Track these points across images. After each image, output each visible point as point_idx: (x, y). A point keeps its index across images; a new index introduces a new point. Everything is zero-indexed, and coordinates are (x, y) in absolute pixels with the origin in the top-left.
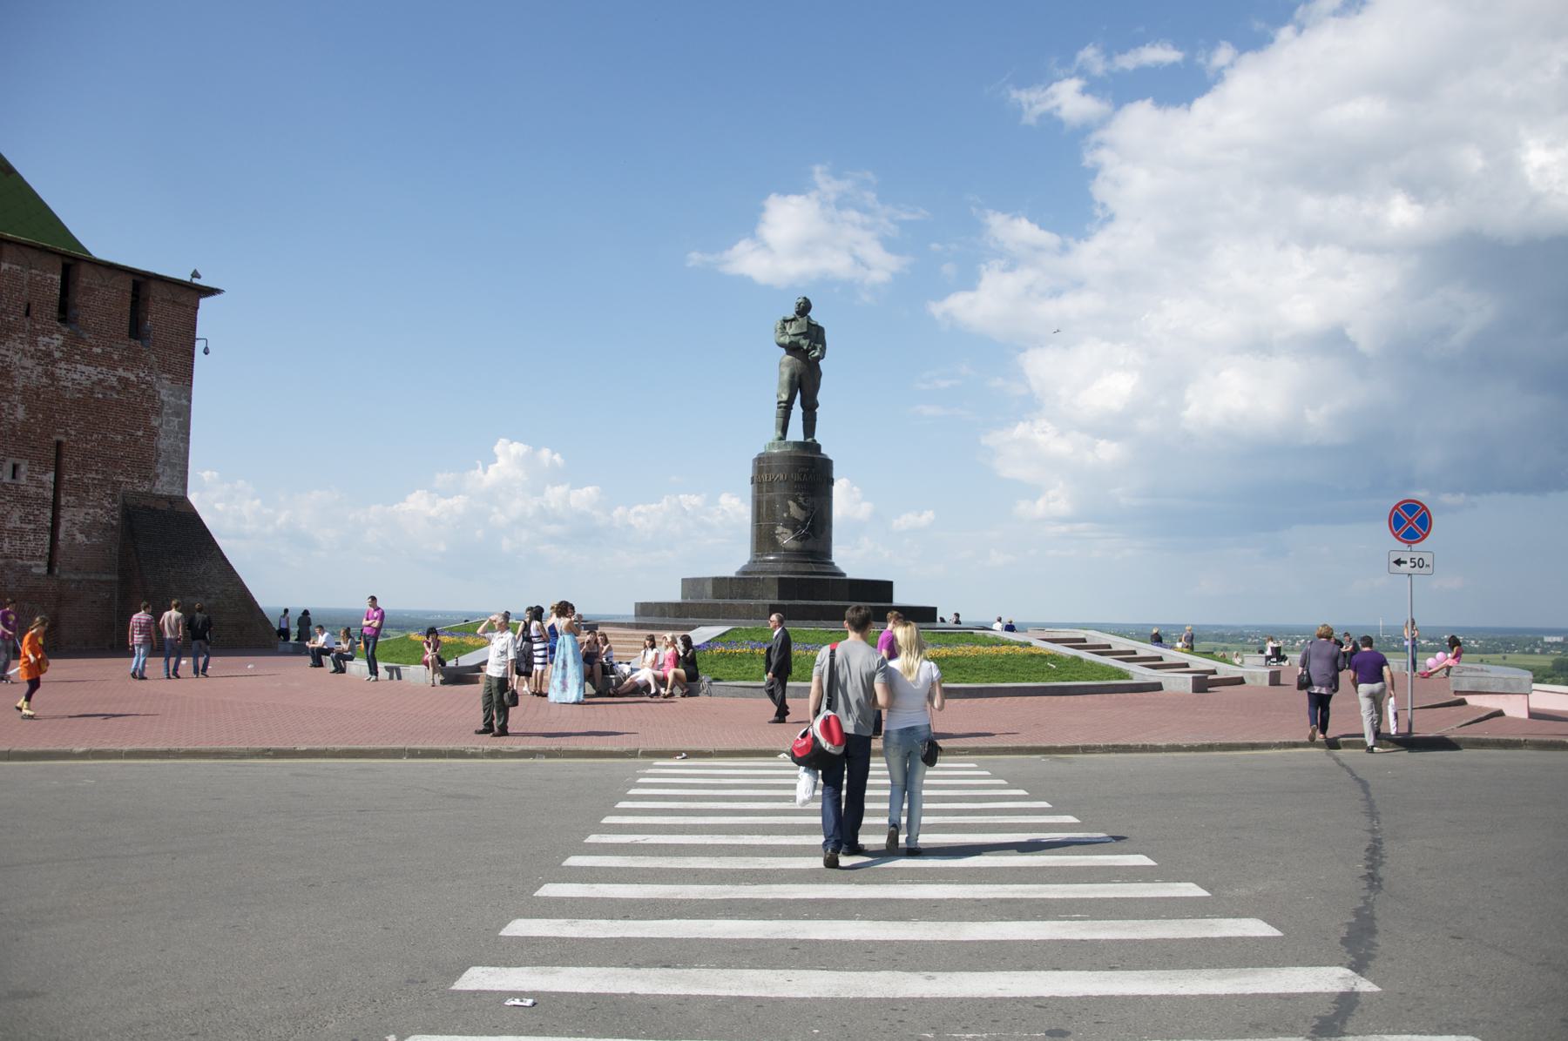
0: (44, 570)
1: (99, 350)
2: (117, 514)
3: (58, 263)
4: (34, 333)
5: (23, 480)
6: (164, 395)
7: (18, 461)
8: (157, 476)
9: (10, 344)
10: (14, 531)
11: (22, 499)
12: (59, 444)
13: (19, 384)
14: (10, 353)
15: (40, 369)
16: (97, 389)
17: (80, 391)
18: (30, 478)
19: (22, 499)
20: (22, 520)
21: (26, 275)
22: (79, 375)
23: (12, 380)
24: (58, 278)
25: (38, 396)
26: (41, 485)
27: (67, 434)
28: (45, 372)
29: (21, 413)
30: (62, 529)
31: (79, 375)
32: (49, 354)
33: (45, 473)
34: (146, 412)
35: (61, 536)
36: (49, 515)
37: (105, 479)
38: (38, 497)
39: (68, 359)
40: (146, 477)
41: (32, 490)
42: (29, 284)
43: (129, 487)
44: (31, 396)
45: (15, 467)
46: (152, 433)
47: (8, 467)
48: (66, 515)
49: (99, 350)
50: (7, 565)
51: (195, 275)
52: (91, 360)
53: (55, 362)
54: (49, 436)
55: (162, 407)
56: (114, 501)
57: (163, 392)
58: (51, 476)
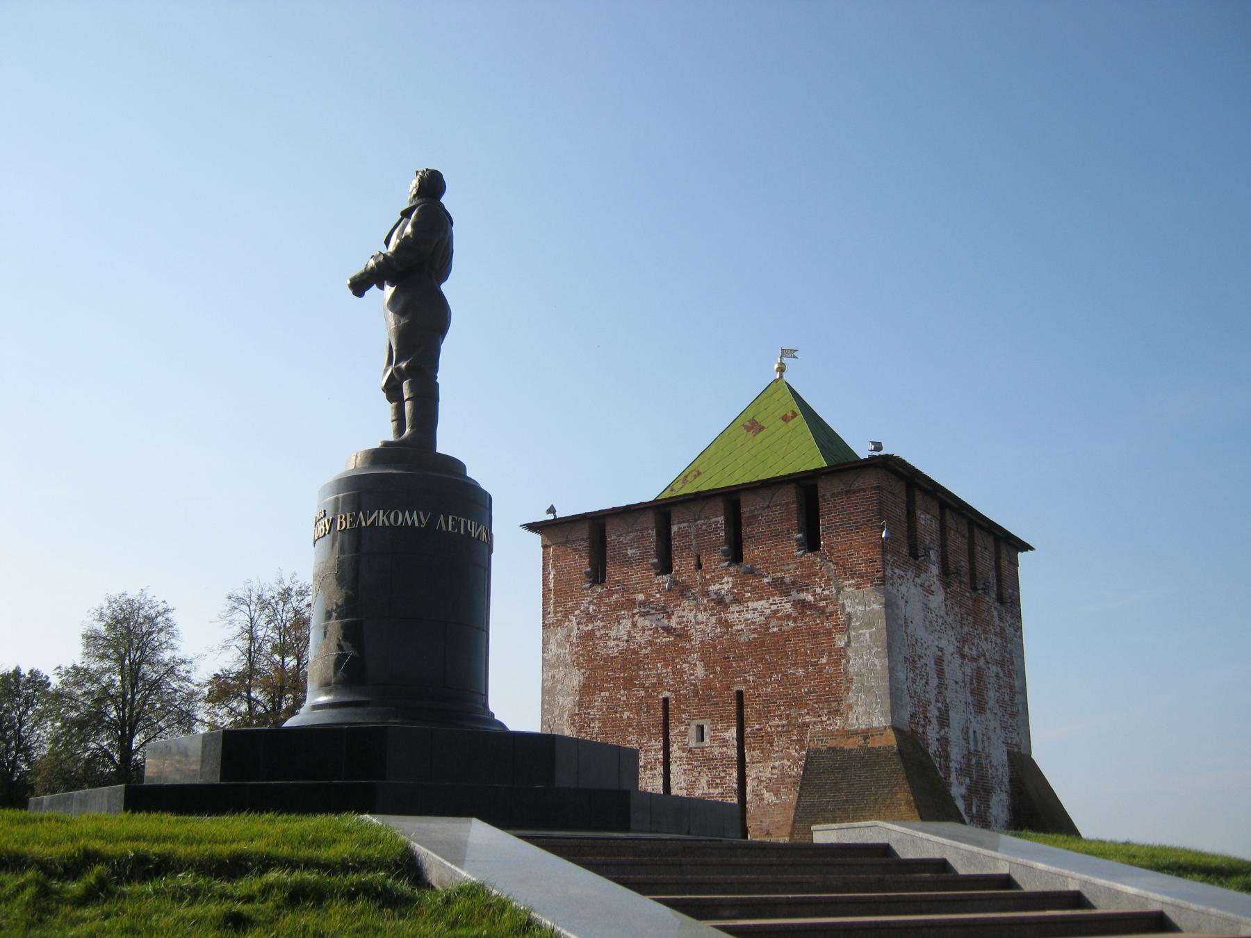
3: (720, 505)
7: (701, 722)
8: (850, 707)
11: (708, 761)
12: (740, 694)
13: (696, 640)
14: (685, 613)
18: (713, 739)
19: (708, 761)
20: (709, 785)
21: (693, 530)
22: (753, 613)
24: (721, 519)
25: (715, 648)
26: (724, 742)
27: (746, 681)
28: (720, 621)
29: (700, 671)
31: (753, 613)
33: (727, 730)
34: (829, 633)
35: (748, 798)
36: (735, 775)
38: (724, 756)
40: (837, 712)
41: (717, 751)
42: (697, 536)
44: (707, 651)
45: (701, 728)
46: (839, 656)
47: (692, 731)
48: (751, 773)
51: (878, 446)
53: (727, 606)
54: (729, 689)
56: (802, 748)
57: (847, 602)
58: (733, 732)
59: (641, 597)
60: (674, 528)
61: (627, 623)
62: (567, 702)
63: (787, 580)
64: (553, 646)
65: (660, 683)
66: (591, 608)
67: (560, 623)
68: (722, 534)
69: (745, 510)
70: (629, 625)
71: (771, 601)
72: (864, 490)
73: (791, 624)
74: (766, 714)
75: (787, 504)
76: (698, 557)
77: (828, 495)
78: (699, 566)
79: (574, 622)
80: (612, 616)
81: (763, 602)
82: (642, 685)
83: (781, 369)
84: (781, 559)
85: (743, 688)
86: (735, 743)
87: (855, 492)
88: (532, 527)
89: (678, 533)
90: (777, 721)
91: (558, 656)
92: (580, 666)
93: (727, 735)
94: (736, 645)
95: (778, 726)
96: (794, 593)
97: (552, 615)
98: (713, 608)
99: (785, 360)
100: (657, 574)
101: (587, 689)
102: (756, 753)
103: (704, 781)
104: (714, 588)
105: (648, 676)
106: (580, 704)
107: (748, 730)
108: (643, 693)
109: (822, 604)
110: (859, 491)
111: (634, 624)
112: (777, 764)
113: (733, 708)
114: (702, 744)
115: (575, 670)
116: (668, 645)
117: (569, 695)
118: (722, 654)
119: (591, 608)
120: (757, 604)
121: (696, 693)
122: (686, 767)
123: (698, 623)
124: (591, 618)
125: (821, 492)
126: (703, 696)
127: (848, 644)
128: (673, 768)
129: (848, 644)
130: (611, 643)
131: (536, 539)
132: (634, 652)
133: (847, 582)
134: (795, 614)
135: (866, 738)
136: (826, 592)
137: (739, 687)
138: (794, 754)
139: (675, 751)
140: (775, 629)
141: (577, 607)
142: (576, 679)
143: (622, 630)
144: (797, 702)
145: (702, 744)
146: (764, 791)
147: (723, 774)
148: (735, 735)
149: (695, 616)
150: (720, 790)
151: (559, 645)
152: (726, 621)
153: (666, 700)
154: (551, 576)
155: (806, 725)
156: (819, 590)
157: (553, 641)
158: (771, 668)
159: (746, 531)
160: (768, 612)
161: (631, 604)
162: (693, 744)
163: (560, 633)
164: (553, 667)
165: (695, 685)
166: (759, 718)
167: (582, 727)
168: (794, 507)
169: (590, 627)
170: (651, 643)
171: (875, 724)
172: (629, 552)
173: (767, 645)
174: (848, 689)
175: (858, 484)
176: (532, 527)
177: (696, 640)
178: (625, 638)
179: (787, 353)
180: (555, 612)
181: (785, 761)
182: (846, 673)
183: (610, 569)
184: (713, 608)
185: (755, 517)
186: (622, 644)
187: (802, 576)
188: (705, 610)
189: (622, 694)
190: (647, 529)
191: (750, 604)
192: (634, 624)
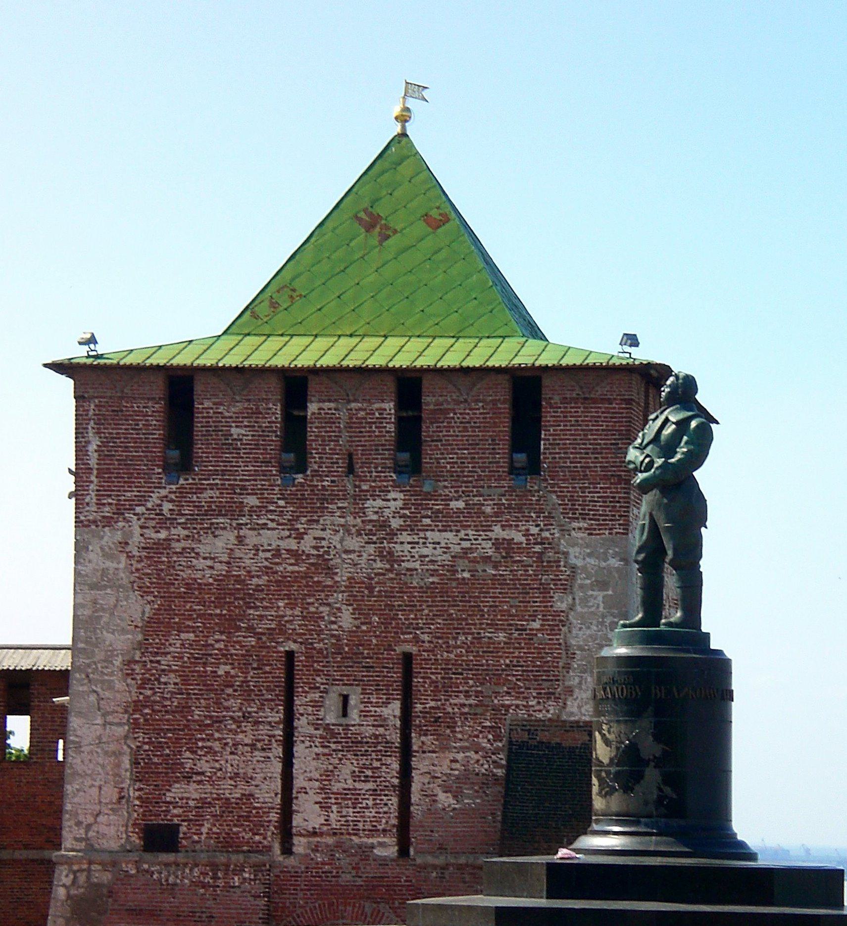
0: (392, 851)
1: (461, 504)
4: (360, 497)
5: (354, 716)
6: (576, 556)
7: (345, 690)
8: (570, 691)
9: (327, 519)
10: (344, 794)
11: (354, 745)
12: (408, 658)
13: (342, 576)
14: (326, 534)
15: (371, 549)
16: (461, 564)
17: (433, 573)
18: (364, 714)
19: (354, 745)
21: (343, 415)
22: (432, 548)
23: (330, 571)
25: (371, 588)
26: (381, 722)
27: (417, 640)
29: (347, 619)
30: (415, 787)
31: (432, 548)
32: (384, 525)
33: (386, 704)
34: (545, 590)
35: (414, 798)
36: (396, 766)
37: (480, 704)
39: (412, 526)
40: (549, 695)
42: (349, 426)
43: (522, 714)
44: (360, 592)
45: (345, 699)
46: (557, 622)
47: (332, 701)
48: (420, 765)
49: (461, 504)
50: (338, 845)
51: (632, 340)
52: (447, 521)
53: (393, 534)
54: (390, 648)
55: (572, 577)
56: (497, 738)
57: (573, 551)
58: (395, 707)
59: (252, 501)
60: (312, 407)
61: (230, 537)
62: (120, 641)
63: (488, 510)
65: (281, 629)
66: (167, 506)
67: (108, 522)
68: (391, 428)
69: (429, 401)
71: (462, 534)
72: (610, 401)
74: (446, 688)
75: (494, 402)
76: (350, 456)
77: (557, 399)
78: (350, 470)
79: (136, 524)
80: (204, 520)
83: (404, 118)
84: (480, 478)
85: (414, 650)
86: (398, 723)
87: (594, 401)
89: (317, 415)
90: (462, 700)
91: (104, 571)
92: (145, 591)
93: (386, 711)
94: (405, 588)
95: (464, 705)
96: (497, 529)
97: (94, 509)
98: (370, 533)
99: (411, 103)
101: (156, 627)
102: (428, 739)
103: (346, 770)
104: (372, 504)
106: (142, 646)
107: (419, 707)
108: (253, 641)
109: (538, 548)
110: (603, 401)
111: (240, 540)
112: (460, 756)
113: (396, 675)
114: (344, 721)
115: (134, 596)
116: (297, 577)
117: (123, 631)
118: (381, 597)
121: (339, 650)
122: (320, 750)
123: (347, 552)
124: (164, 522)
125: (546, 393)
126: (350, 657)
127: (572, 608)
128: (299, 749)
129: (572, 608)
130: (201, 563)
131: (67, 384)
132: (238, 580)
133: (575, 525)
134: (496, 557)
136: (546, 534)
140: (466, 575)
141: (142, 500)
142: (136, 608)
143: (220, 544)
144: (497, 678)
145: (344, 721)
146: (439, 791)
148: (398, 713)
149: (342, 541)
150: (370, 786)
151: (107, 556)
152: (390, 553)
153: (290, 655)
154: (92, 447)
156: (534, 530)
157: (95, 547)
159: (428, 430)
160: (457, 549)
161: (234, 510)
162: (331, 719)
163: (110, 537)
164: (94, 587)
165: (338, 638)
166: (436, 691)
167: (145, 681)
168: (505, 408)
169: (163, 535)
170: (267, 571)
172: (234, 431)
174: (567, 667)
175: (600, 391)
177: (342, 576)
178: (225, 558)
179: (414, 90)
180: (100, 504)
181: (471, 754)
182: (567, 647)
183: (199, 448)
184: (370, 533)
185: (447, 411)
186: (217, 566)
187: (510, 507)
188: (359, 534)
190: (267, 400)
191: (428, 534)
192: (240, 540)
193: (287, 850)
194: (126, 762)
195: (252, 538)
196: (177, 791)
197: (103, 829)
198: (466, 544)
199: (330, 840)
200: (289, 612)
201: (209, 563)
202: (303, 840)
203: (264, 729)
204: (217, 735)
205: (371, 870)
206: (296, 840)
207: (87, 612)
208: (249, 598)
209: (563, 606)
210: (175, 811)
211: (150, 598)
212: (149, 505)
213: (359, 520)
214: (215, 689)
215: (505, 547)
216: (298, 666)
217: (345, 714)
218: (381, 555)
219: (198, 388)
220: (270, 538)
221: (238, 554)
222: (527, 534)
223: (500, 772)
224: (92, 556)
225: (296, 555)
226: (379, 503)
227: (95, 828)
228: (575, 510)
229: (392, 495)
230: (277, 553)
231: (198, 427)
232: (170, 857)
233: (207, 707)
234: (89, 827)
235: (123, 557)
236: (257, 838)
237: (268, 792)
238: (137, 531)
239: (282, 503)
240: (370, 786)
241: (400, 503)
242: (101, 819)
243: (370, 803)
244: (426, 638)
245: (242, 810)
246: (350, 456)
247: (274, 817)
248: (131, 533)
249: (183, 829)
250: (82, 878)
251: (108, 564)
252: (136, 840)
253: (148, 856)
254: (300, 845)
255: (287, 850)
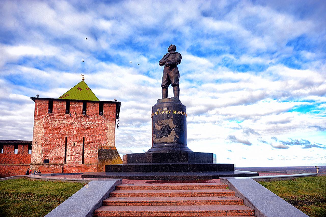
0: (81, 163)
1: (92, 119)
2: (98, 151)
4: (77, 117)
5: (76, 145)
6: (108, 126)
12: (84, 138)
13: (75, 127)
14: (72, 122)
25: (79, 129)
27: (85, 136)
29: (75, 133)
30: (85, 155)
32: (81, 121)
36: (82, 152)
39: (85, 121)
41: (78, 148)
42: (76, 108)
43: (100, 145)
44: (77, 129)
45: (74, 143)
46: (106, 133)
47: (73, 143)
48: (85, 152)
49: (92, 119)
50: (73, 162)
58: (82, 144)
59: (61, 117)
60: (71, 105)
64: (37, 124)
67: (39, 119)
70: (58, 122)
71: (92, 122)
73: (96, 127)
74: (90, 142)
76: (76, 112)
78: (76, 113)
80: (54, 119)
81: (90, 122)
82: (61, 134)
85: (85, 137)
86: (82, 146)
88: (33, 99)
89: (71, 106)
91: (39, 126)
94: (84, 129)
100: (66, 113)
101: (46, 133)
103: (74, 153)
105: (62, 132)
106: (44, 136)
107: (85, 144)
111: (59, 122)
114: (74, 146)
116: (67, 127)
118: (80, 130)
119: (48, 117)
120: (88, 122)
126: (75, 137)
127: (108, 132)
128: (67, 150)
129: (108, 132)
130: (53, 125)
132: (59, 127)
133: (108, 122)
135: (110, 148)
137: (84, 137)
138: (95, 149)
139: (68, 147)
140: (93, 127)
143: (56, 122)
144: (97, 141)
146: (88, 155)
147: (79, 152)
148: (82, 145)
150: (78, 155)
152: (82, 125)
154: (37, 109)
155: (98, 145)
156: (102, 122)
158: (92, 134)
159: (87, 109)
165: (74, 135)
169: (48, 121)
171: (112, 146)
172: (59, 108)
173: (90, 129)
176: (33, 99)
177: (75, 127)
180: (38, 117)
183: (54, 110)
189: (56, 135)
191: (87, 122)
192: (59, 122)
193: (65, 163)
194: (41, 151)
195: (61, 122)
196: (49, 155)
197: (37, 160)
198: (92, 124)
199: (72, 162)
200: (66, 132)
201: (54, 125)
202: (68, 162)
203: (62, 147)
204: (55, 148)
205: (78, 165)
206: (67, 162)
207: (36, 131)
208: (60, 130)
209: (106, 132)
210: (49, 158)
211: (45, 129)
212: (46, 117)
213: (77, 120)
214: (55, 142)
215: (98, 124)
216: (67, 139)
217: (74, 145)
218: (80, 125)
219: (54, 102)
220: (64, 122)
221: (59, 124)
222: (101, 122)
223: (97, 153)
224: (37, 123)
225: (67, 124)
226: (80, 118)
227: (36, 160)
228: (108, 120)
229: (82, 117)
230: (65, 124)
231: (53, 107)
232: (48, 164)
233: (54, 144)
234: (35, 160)
235: (41, 124)
236: (61, 161)
237: (63, 156)
238: (44, 120)
239: (66, 117)
240: (78, 155)
241: (83, 118)
242: (37, 159)
243: (78, 157)
244: (87, 135)
245: (59, 158)
246: (76, 112)
247: (64, 159)
248: (43, 121)
249: (49, 160)
250: (34, 167)
251: (39, 125)
252: (43, 162)
253: (44, 164)
254: (67, 162)
255: (65, 163)
